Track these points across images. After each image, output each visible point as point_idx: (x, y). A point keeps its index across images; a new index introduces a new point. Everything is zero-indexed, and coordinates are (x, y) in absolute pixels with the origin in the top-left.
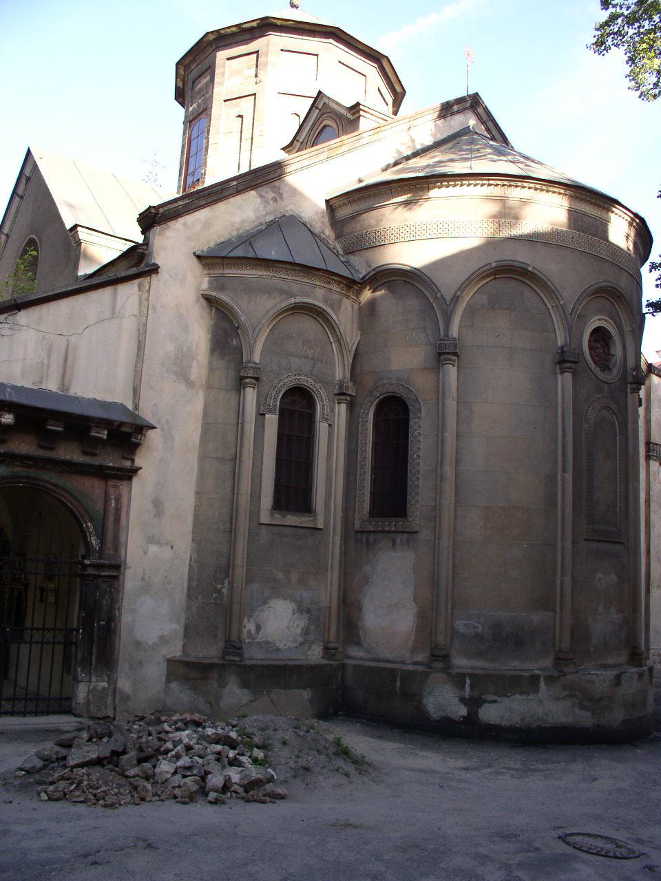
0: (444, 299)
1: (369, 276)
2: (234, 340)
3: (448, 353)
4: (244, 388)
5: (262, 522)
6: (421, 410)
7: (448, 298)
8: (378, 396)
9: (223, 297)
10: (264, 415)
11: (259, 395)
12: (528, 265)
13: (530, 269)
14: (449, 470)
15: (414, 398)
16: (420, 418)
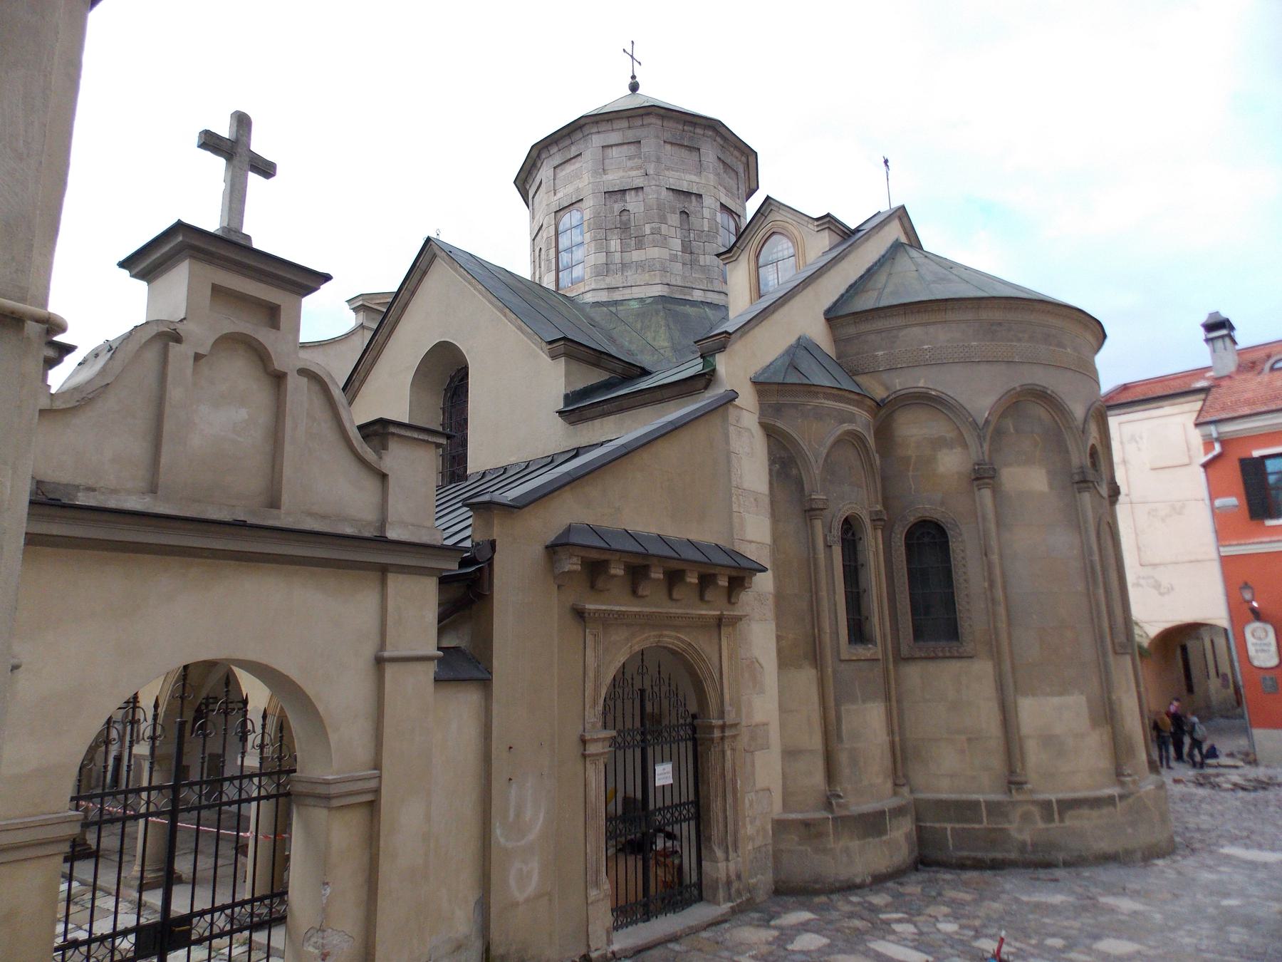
0: (977, 424)
1: (889, 399)
2: (793, 469)
3: (988, 478)
4: (811, 520)
5: (843, 658)
6: (961, 535)
7: (981, 422)
8: (912, 519)
9: (779, 424)
10: (831, 546)
11: (823, 526)
12: (1047, 389)
13: (1049, 392)
14: (999, 594)
15: (953, 521)
16: (963, 541)
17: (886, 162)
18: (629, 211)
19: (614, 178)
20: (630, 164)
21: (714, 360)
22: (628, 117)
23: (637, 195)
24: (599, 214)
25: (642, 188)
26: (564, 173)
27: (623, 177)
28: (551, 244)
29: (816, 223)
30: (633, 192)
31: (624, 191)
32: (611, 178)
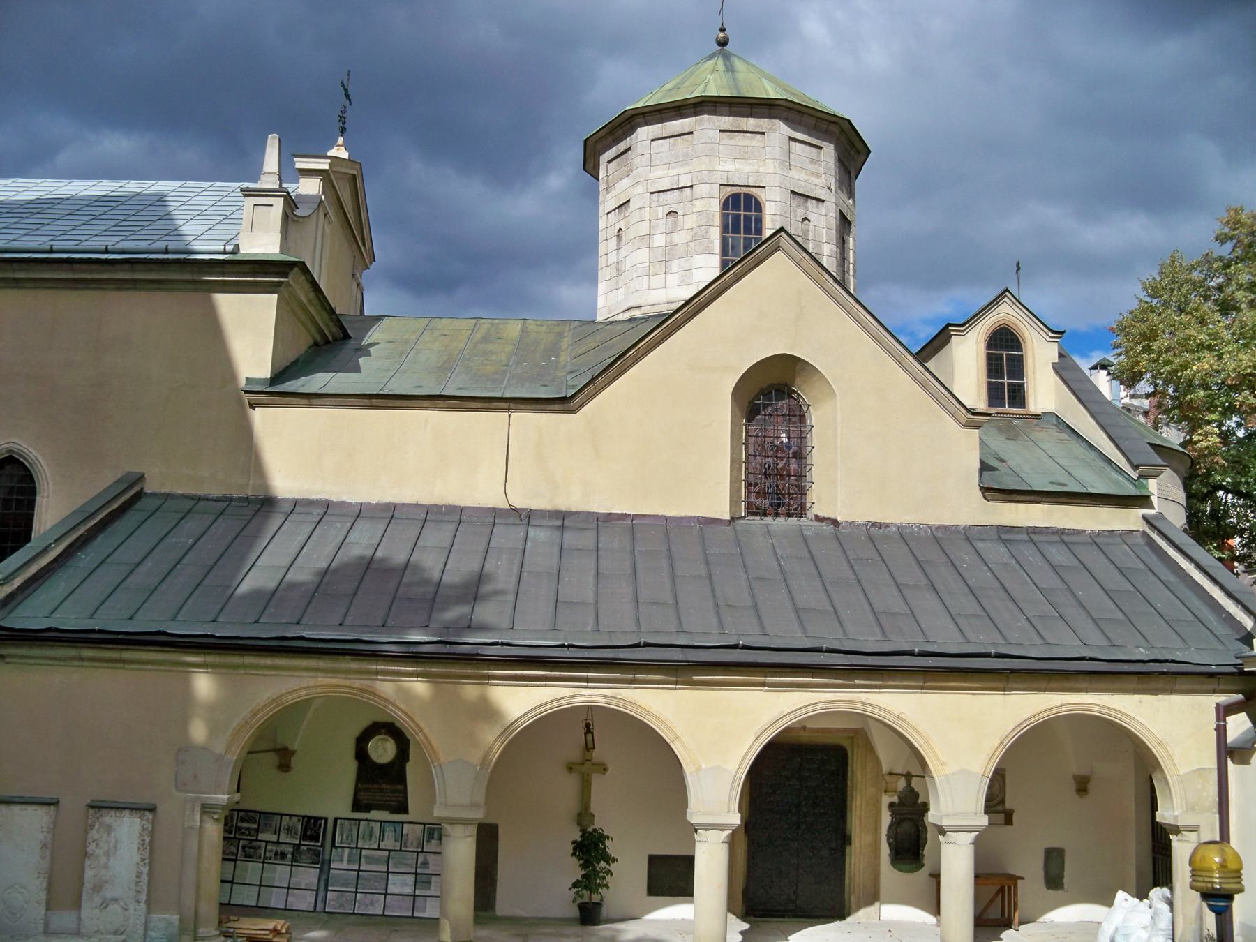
17: (1018, 265)
18: (809, 221)
19: (803, 179)
20: (811, 167)
21: (1147, 484)
22: (818, 118)
23: (817, 207)
24: (785, 213)
25: (823, 201)
26: (733, 142)
27: (806, 181)
28: (713, 220)
29: (1051, 334)
30: (814, 201)
31: (807, 197)
32: (797, 177)
